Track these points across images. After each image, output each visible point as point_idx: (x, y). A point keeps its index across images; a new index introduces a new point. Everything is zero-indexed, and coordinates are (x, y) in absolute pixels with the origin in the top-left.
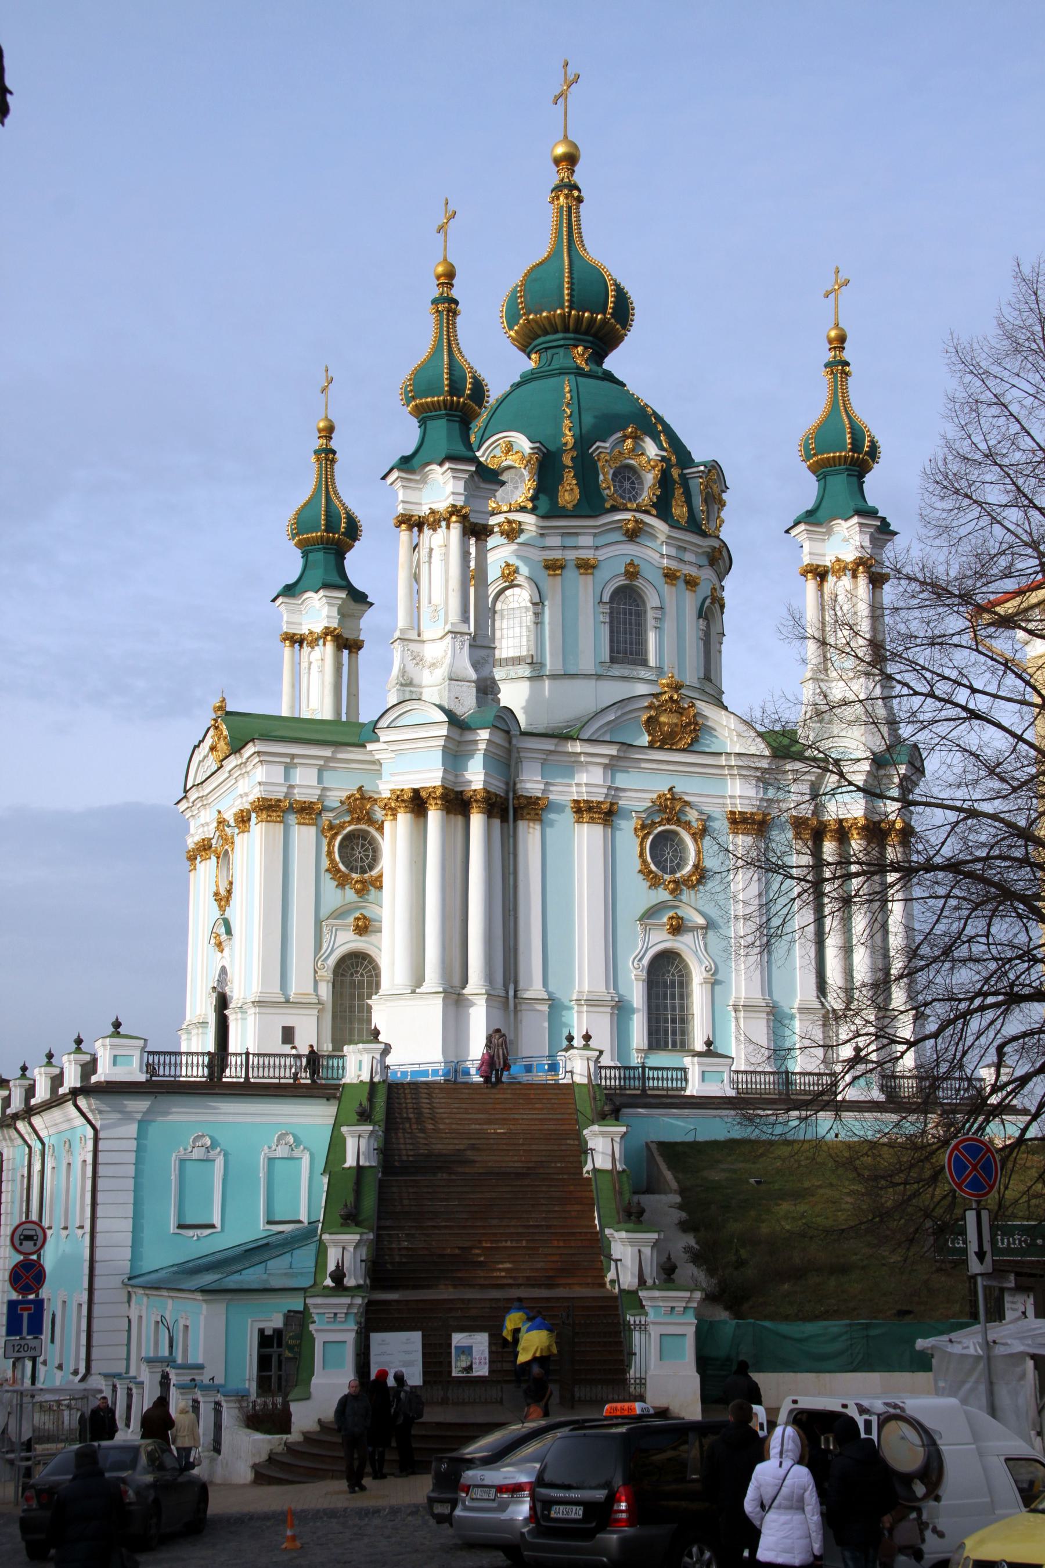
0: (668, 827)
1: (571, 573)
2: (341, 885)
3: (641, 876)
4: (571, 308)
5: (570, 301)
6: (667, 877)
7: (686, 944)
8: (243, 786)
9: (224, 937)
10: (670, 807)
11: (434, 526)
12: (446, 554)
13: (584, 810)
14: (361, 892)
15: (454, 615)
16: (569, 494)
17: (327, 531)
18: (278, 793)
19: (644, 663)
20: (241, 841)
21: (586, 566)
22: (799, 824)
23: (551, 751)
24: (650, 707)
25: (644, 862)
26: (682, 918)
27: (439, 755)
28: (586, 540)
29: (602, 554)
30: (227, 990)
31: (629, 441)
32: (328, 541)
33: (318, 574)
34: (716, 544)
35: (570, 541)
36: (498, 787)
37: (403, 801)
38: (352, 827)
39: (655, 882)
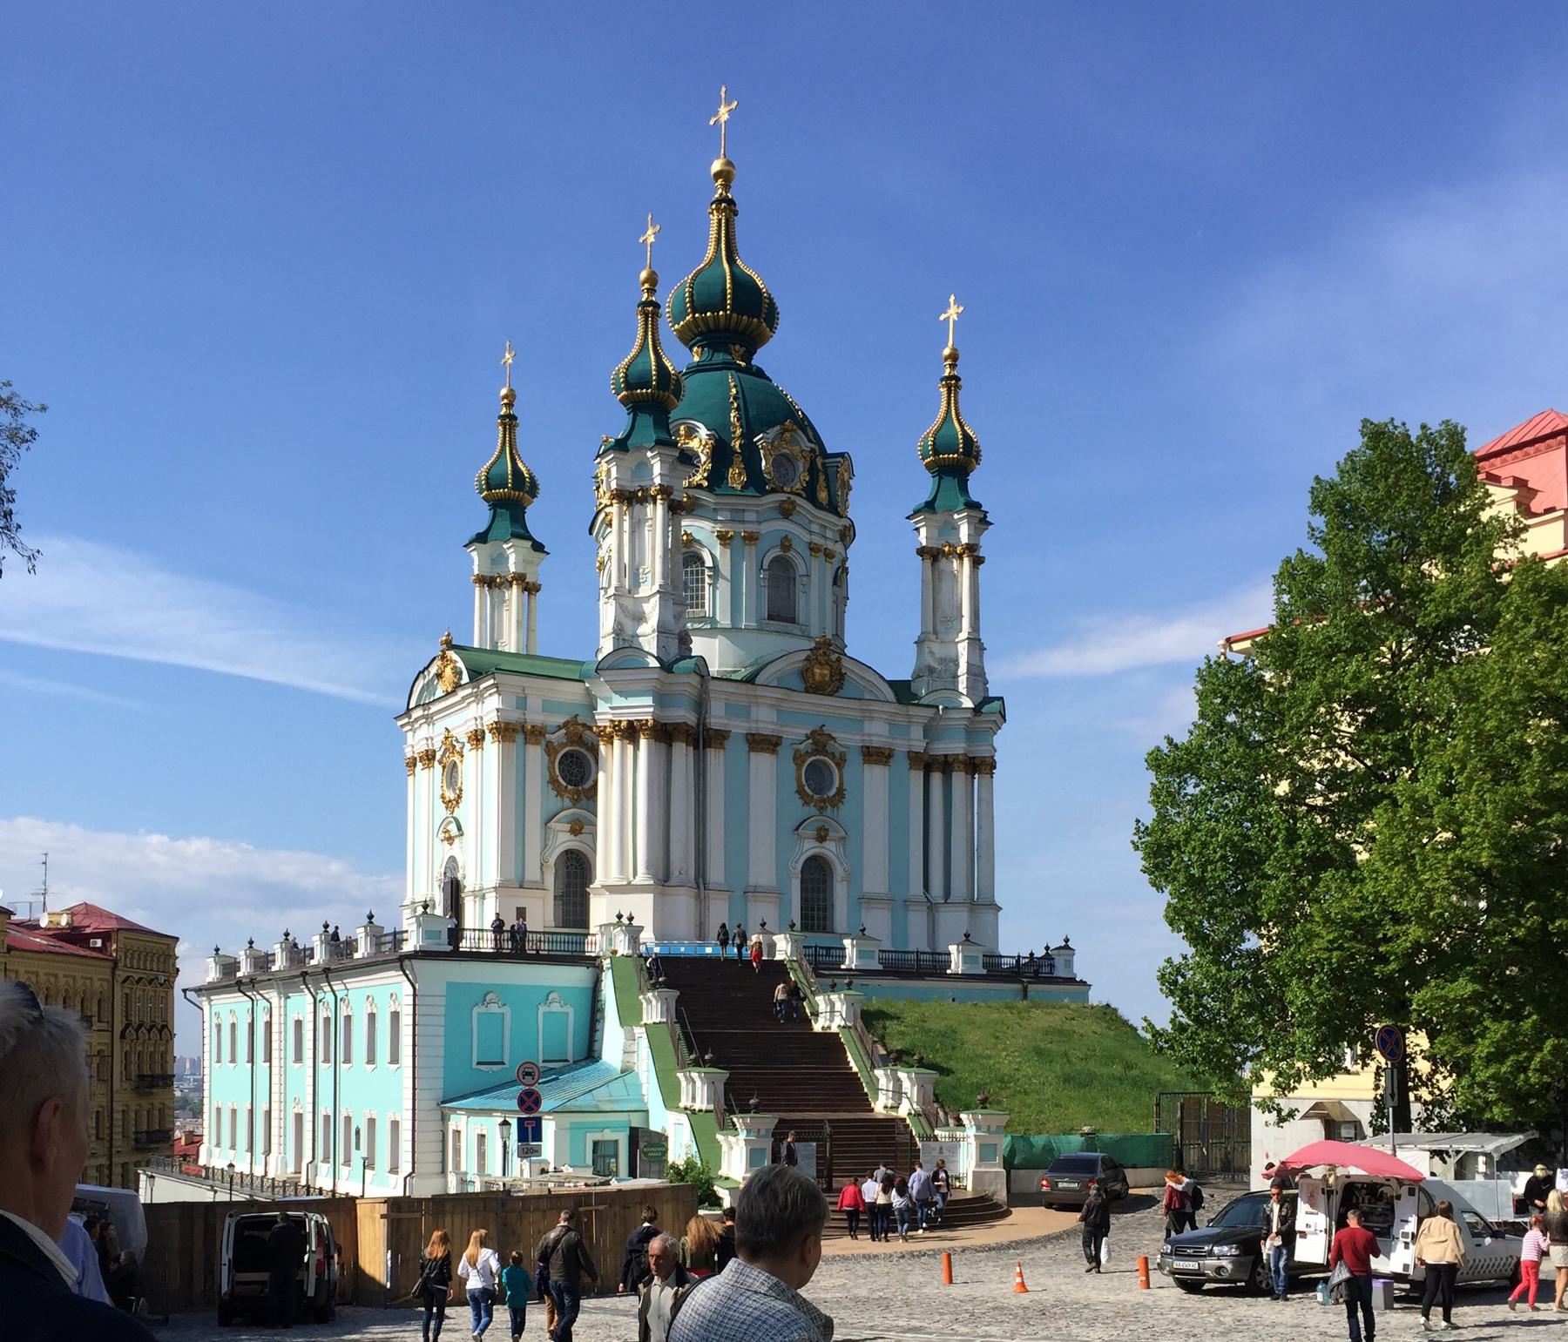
1: (737, 542)
2: (559, 794)
7: (830, 849)
8: (474, 710)
9: (453, 828)
10: (820, 740)
14: (575, 803)
15: (659, 580)
18: (515, 716)
19: (793, 620)
20: (470, 755)
21: (751, 538)
24: (807, 659)
28: (750, 516)
29: (765, 528)
30: (459, 876)
32: (510, 499)
34: (848, 523)
35: (737, 517)
36: (690, 718)
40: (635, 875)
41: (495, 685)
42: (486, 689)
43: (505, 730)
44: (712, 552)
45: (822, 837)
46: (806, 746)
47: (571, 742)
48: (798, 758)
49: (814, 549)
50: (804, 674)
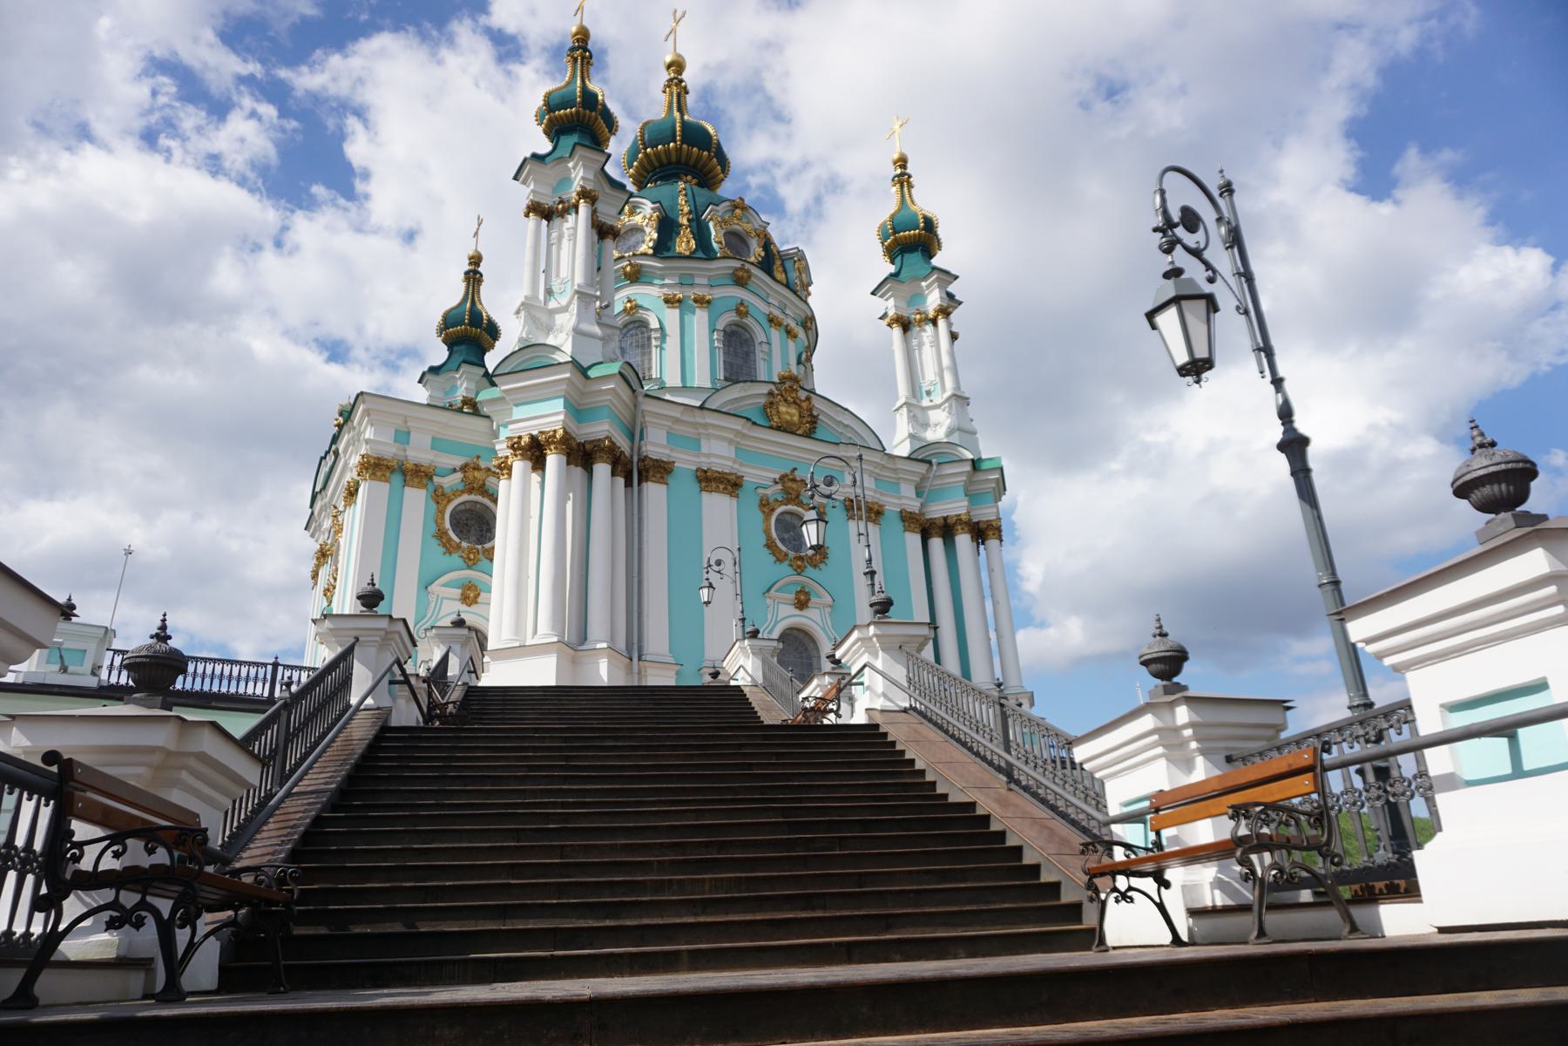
0: (790, 507)
3: (767, 551)
4: (683, 142)
5: (683, 136)
6: (792, 554)
7: (813, 619)
10: (791, 487)
11: (563, 213)
12: (575, 235)
13: (709, 480)
15: (579, 279)
16: (684, 243)
17: (471, 324)
18: (389, 450)
22: (910, 520)
23: (677, 421)
24: (771, 393)
25: (769, 537)
26: (807, 594)
27: (561, 401)
31: (738, 211)
33: (458, 358)
36: (623, 443)
37: (520, 448)
38: (465, 497)
39: (780, 558)
40: (535, 632)
41: (367, 412)
42: (360, 423)
43: (375, 467)
44: (658, 315)
45: (802, 603)
46: (774, 492)
47: (470, 491)
48: (766, 506)
49: (772, 320)
50: (769, 408)
